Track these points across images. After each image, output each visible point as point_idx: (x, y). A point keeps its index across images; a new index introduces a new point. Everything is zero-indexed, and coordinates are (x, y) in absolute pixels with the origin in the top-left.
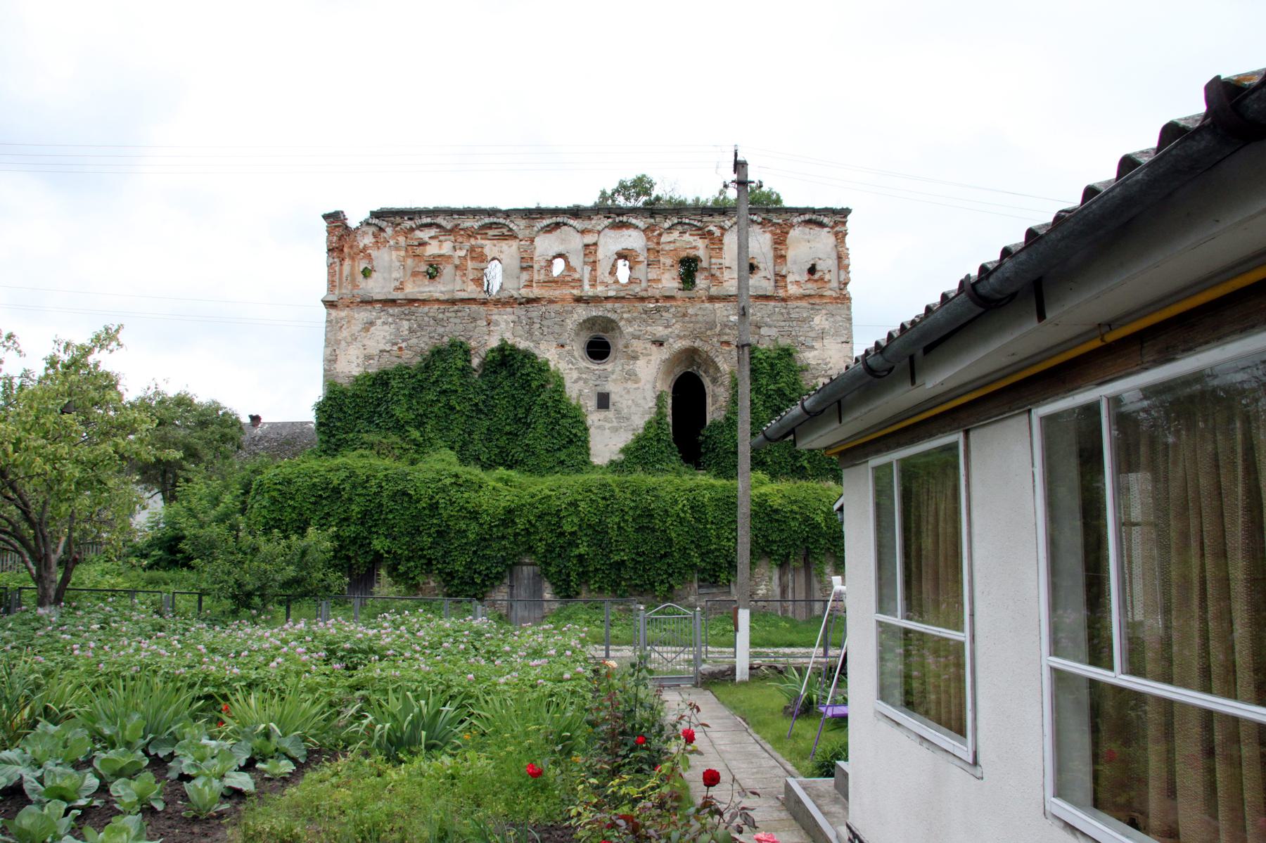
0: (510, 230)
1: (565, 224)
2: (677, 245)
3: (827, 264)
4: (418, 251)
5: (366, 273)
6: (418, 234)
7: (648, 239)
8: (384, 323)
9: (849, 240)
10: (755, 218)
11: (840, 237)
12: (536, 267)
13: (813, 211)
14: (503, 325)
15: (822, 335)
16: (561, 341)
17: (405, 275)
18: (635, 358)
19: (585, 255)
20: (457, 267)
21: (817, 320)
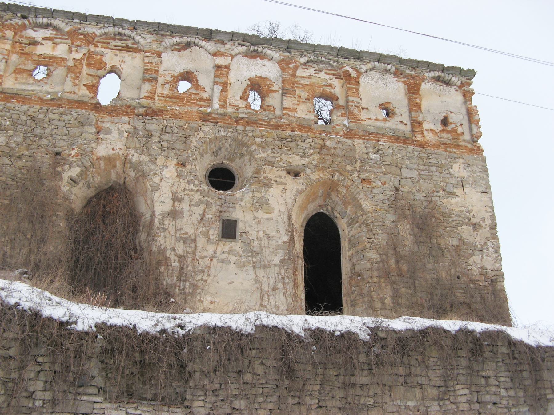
0: (135, 43)
2: (313, 80)
3: (458, 117)
4: (27, 49)
6: (30, 33)
7: (283, 70)
9: (475, 100)
11: (467, 95)
12: (161, 80)
13: (443, 69)
14: (115, 134)
15: (462, 183)
17: (5, 71)
18: (268, 185)
19: (215, 76)
20: (69, 69)
21: (456, 167)
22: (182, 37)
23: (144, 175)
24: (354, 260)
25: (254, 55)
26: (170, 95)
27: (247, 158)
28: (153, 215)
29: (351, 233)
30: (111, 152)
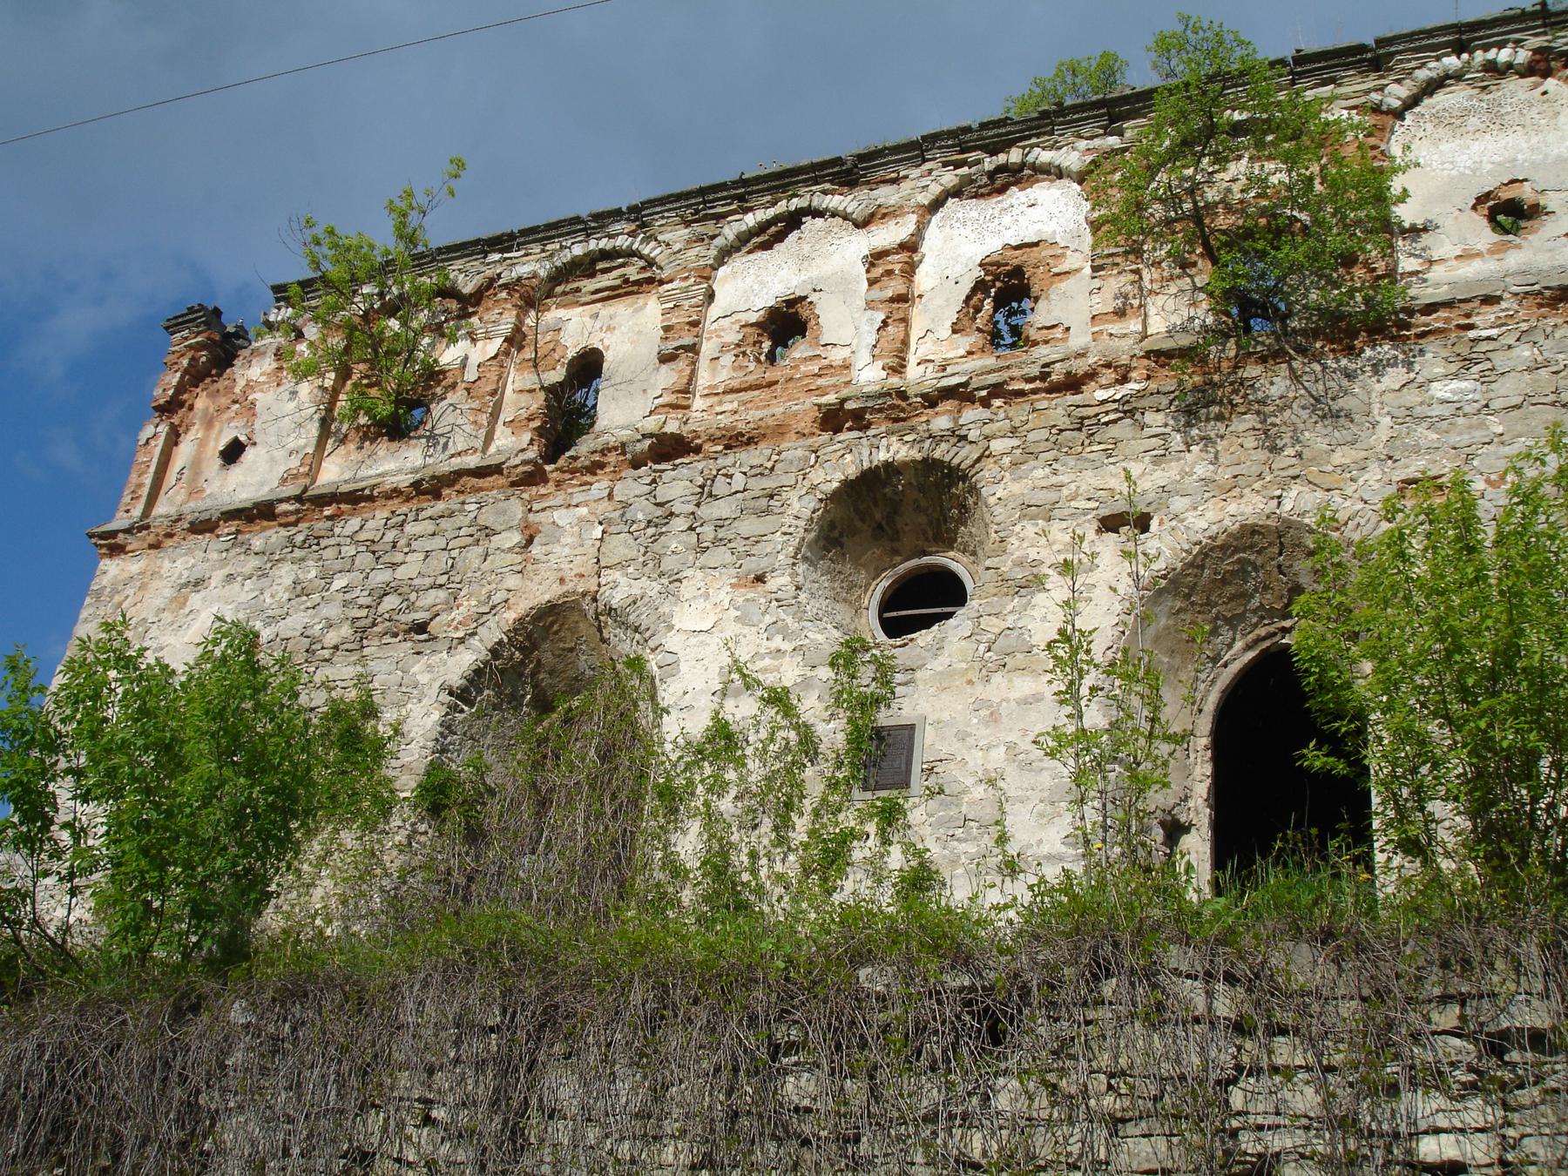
0: (651, 263)
1: (817, 213)
5: (233, 453)
10: (1504, 55)
12: (708, 348)
16: (752, 565)
22: (774, 204)
26: (735, 384)
30: (560, 590)
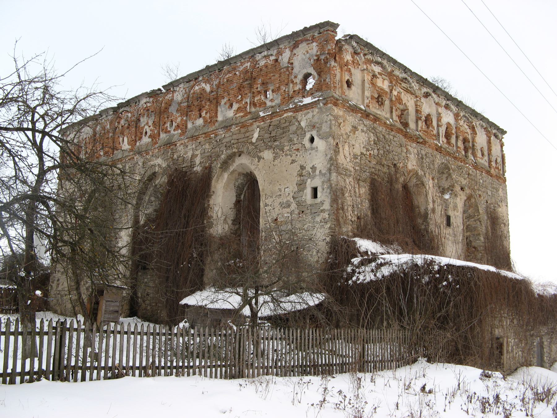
8: (363, 131)
11: (502, 145)
23: (423, 184)
24: (471, 239)
25: (447, 107)
27: (445, 176)
28: (426, 209)
29: (468, 223)
